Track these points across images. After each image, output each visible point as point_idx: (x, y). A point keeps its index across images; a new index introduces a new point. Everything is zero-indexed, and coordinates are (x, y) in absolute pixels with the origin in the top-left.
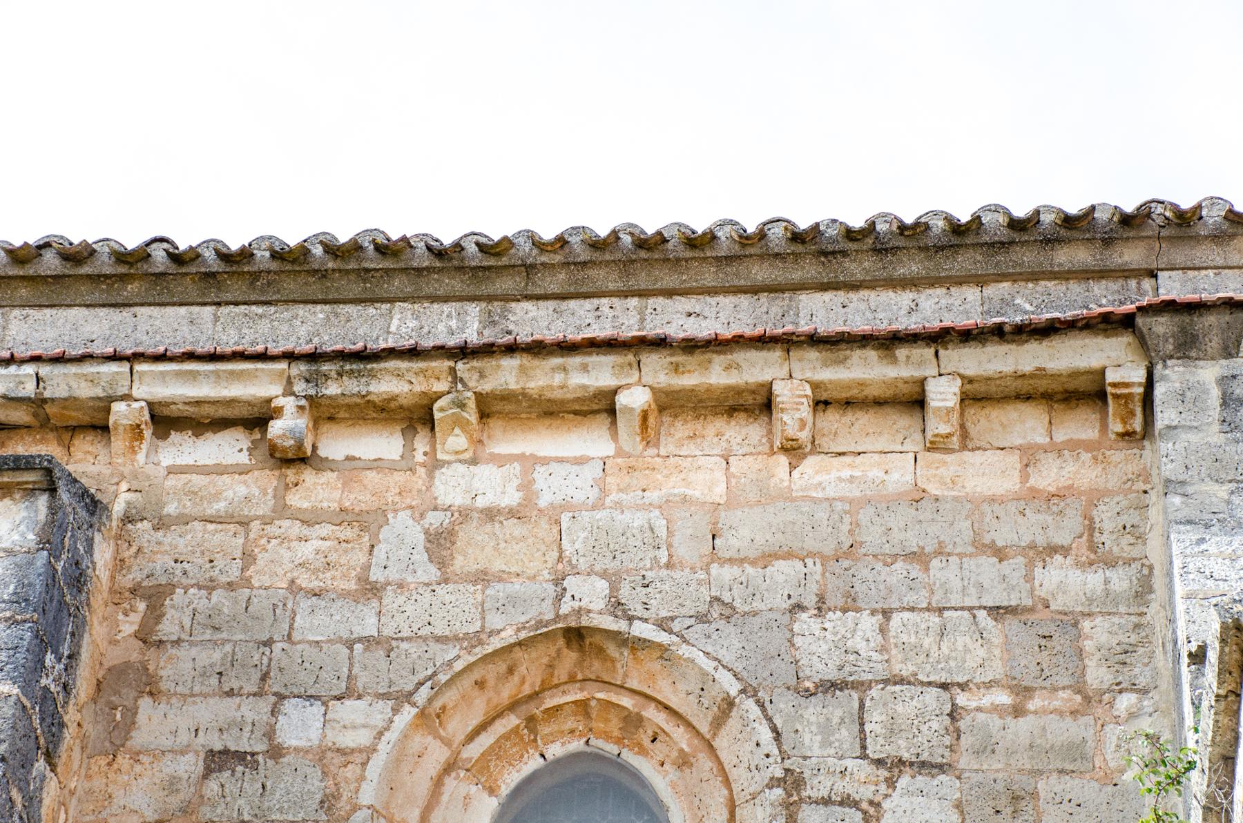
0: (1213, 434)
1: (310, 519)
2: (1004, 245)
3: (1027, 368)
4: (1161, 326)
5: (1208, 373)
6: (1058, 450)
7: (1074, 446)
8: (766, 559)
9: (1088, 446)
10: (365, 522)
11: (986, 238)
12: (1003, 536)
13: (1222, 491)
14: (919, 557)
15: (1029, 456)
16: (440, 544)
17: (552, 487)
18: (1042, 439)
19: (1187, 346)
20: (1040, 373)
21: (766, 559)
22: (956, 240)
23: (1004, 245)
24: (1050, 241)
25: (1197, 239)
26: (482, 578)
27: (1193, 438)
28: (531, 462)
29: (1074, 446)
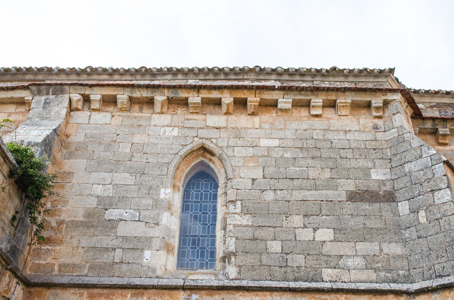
0: (40, 109)
2: (15, 74)
3: (9, 96)
4: (34, 88)
5: (43, 98)
6: (16, 113)
7: (19, 112)
9: (22, 112)
11: (12, 73)
13: (38, 119)
15: (10, 114)
18: (13, 111)
19: (39, 93)
20: (12, 98)
22: (5, 73)
23: (15, 74)
24: (24, 74)
25: (53, 74)
27: (36, 110)
29: (19, 112)
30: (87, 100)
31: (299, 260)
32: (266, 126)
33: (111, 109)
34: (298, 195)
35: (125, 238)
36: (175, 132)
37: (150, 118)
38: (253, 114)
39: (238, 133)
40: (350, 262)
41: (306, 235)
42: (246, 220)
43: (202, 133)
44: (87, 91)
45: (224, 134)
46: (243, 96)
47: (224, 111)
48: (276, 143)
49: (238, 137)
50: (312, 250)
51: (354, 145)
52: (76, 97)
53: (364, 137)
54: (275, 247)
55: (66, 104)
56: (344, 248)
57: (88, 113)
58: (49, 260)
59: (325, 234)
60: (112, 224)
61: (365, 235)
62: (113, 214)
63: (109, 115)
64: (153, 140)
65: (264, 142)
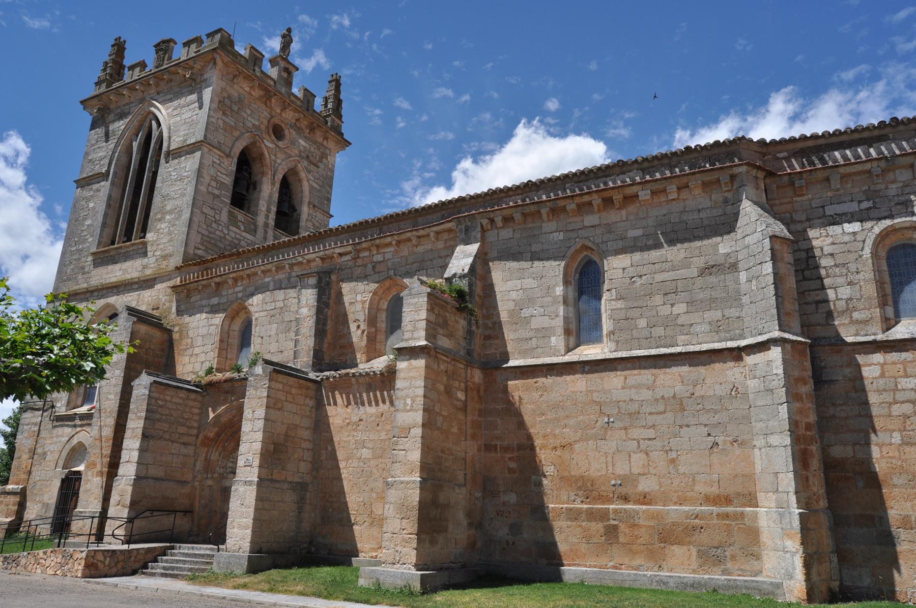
1: (359, 266)
8: (413, 263)
10: (365, 266)
12: (442, 255)
14: (431, 260)
16: (374, 267)
17: (388, 256)
21: (413, 263)
26: (379, 272)
28: (384, 253)
30: (492, 221)
31: (659, 331)
32: (632, 217)
33: (511, 224)
34: (659, 277)
35: (537, 330)
36: (561, 236)
37: (541, 227)
38: (620, 208)
39: (609, 228)
40: (698, 328)
41: (665, 310)
42: (620, 304)
43: (583, 233)
44: (492, 215)
45: (599, 231)
46: (609, 195)
47: (596, 210)
48: (639, 232)
49: (610, 232)
50: (670, 322)
51: (706, 222)
52: (485, 222)
53: (715, 212)
54: (642, 323)
55: (479, 228)
56: (695, 318)
57: (496, 231)
58: (493, 351)
59: (680, 308)
60: (527, 320)
61: (712, 303)
62: (526, 313)
63: (511, 230)
64: (546, 247)
65: (632, 233)
